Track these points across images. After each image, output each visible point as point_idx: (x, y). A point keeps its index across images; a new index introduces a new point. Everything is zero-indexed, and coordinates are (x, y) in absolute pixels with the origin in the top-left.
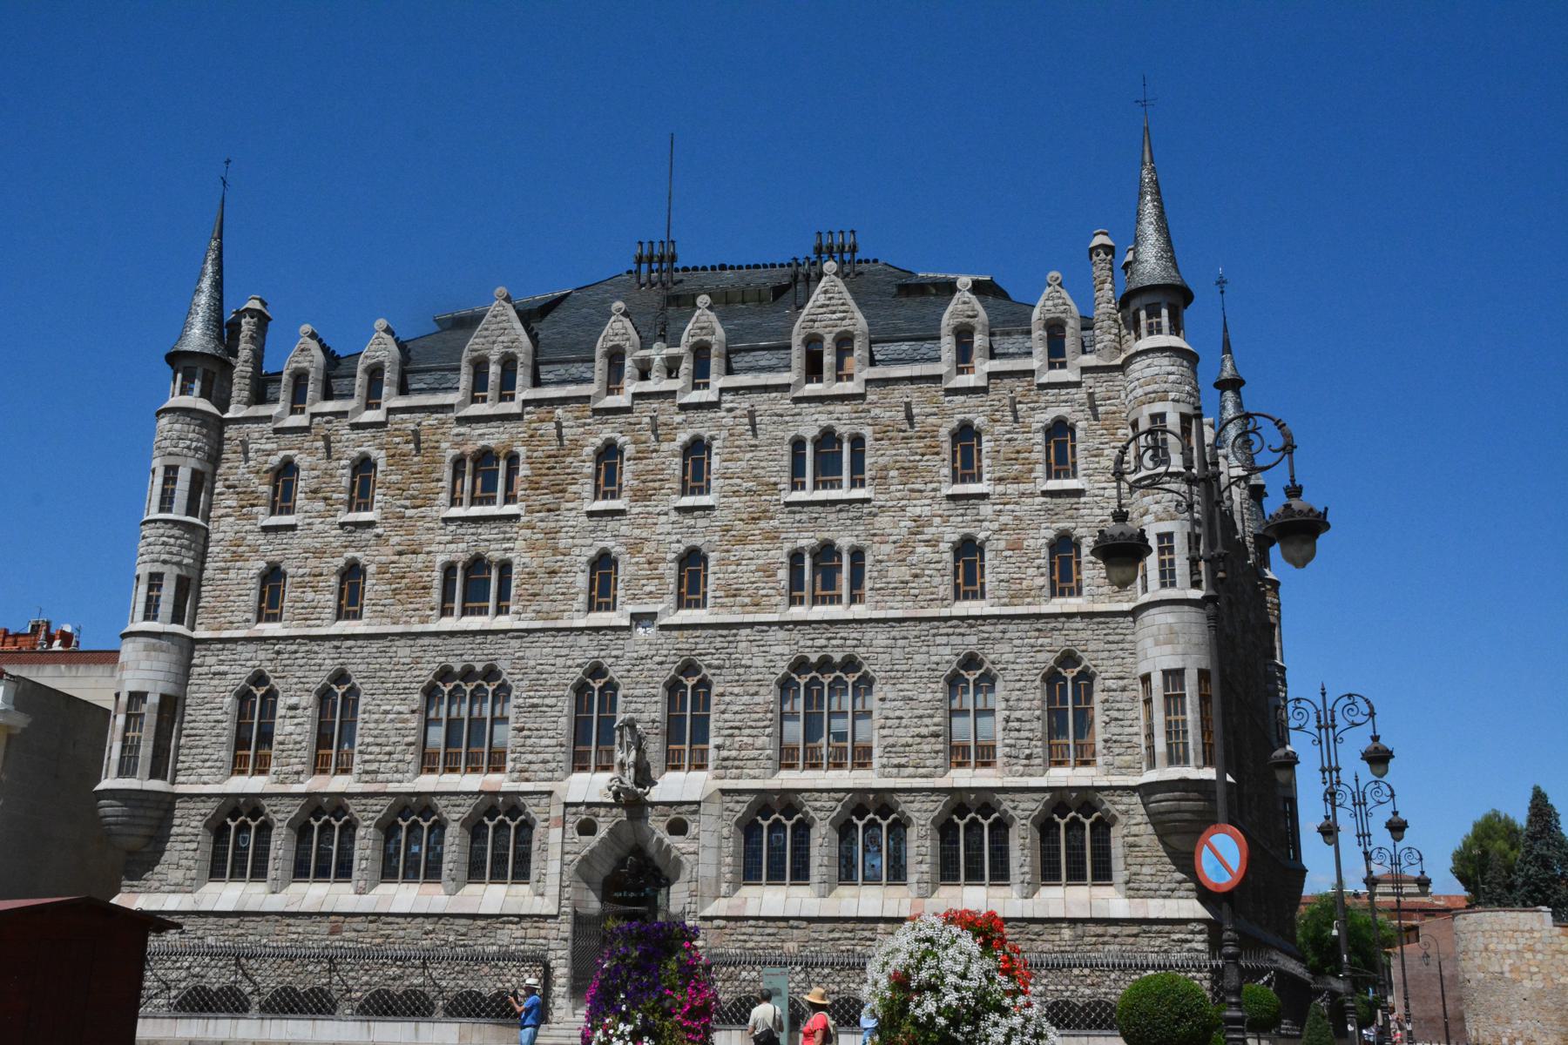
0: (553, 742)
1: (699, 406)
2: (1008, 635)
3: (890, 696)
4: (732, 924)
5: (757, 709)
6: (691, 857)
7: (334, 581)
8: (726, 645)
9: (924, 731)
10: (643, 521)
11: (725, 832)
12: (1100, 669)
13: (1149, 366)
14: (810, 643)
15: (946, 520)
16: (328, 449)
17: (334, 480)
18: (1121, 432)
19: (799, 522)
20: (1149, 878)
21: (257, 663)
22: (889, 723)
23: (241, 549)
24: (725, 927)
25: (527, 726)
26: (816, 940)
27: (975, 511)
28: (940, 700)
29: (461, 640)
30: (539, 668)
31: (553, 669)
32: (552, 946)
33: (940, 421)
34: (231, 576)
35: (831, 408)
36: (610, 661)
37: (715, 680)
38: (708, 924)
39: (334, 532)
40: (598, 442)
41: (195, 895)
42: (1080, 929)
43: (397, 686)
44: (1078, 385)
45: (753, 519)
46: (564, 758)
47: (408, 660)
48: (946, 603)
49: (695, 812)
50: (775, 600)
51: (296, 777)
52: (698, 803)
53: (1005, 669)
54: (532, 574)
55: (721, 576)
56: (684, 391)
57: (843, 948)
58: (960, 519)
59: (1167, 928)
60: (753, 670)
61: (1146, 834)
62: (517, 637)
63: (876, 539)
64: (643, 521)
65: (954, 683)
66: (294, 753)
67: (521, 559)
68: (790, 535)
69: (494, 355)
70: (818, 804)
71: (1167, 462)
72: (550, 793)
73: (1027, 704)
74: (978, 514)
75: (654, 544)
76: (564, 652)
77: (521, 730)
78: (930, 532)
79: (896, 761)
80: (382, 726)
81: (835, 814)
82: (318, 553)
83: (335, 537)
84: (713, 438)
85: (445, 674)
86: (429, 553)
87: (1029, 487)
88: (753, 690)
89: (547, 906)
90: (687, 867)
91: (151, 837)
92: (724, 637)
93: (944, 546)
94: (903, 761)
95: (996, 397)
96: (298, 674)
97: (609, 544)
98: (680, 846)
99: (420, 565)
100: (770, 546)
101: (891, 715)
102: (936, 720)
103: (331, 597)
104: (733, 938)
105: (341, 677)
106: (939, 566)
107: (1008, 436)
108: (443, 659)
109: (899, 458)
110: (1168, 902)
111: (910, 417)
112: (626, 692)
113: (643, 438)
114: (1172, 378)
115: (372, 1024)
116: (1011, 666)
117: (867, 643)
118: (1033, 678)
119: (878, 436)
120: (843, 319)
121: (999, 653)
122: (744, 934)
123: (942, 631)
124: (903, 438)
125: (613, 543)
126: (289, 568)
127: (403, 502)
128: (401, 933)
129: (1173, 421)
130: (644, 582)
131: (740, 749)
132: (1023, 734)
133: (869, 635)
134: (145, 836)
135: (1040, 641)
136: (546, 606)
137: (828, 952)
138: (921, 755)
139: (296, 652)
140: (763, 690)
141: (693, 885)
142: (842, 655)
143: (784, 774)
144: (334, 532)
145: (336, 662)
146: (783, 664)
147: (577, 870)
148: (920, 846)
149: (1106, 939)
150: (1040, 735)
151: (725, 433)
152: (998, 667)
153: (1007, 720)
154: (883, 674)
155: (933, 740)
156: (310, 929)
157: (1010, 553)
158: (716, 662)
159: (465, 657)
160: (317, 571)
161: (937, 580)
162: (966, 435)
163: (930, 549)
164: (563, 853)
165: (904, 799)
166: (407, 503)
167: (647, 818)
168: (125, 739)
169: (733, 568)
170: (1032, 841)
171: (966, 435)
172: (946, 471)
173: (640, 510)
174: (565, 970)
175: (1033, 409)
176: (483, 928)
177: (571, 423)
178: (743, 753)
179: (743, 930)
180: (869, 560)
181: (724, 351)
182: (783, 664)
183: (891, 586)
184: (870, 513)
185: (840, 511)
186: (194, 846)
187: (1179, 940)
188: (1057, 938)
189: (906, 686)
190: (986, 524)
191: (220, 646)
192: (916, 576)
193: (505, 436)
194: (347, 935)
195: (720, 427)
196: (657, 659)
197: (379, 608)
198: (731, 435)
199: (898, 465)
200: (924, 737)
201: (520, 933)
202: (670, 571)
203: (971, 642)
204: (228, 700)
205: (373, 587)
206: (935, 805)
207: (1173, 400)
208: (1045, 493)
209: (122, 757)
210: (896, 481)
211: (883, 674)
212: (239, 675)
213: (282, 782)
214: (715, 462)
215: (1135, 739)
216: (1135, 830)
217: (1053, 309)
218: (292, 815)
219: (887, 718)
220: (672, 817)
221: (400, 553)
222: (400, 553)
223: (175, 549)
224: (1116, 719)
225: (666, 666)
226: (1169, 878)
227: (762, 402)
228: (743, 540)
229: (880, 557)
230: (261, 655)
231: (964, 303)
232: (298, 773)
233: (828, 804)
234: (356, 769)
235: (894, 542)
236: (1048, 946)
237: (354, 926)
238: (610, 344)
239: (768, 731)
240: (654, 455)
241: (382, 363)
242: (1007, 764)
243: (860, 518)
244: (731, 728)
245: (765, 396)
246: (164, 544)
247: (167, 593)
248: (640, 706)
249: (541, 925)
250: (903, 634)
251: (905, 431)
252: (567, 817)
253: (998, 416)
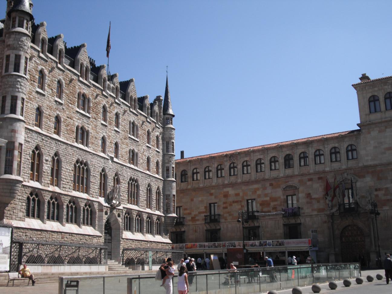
17: (54, 84)
21: (37, 141)
34: (29, 105)
36: (106, 168)
43: (70, 161)
62: (91, 155)
82: (50, 108)
83: (54, 105)
86: (74, 120)
92: (122, 167)
100: (127, 147)
108: (78, 156)
115: (91, 266)
121: (152, 184)
145: (57, 148)
156: (57, 237)
191: (28, 131)
194: (66, 239)
202: (113, 146)
213: (44, 186)
222: (68, 117)
228: (123, 143)
230: (39, 139)
232: (48, 184)
240: (111, 113)
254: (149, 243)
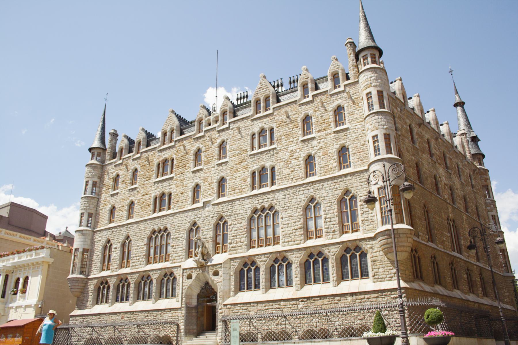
0: (182, 249)
1: (223, 130)
2: (324, 187)
3: (284, 216)
4: (233, 307)
5: (242, 228)
7: (126, 208)
8: (231, 207)
9: (296, 227)
10: (207, 171)
11: (232, 274)
12: (358, 193)
13: (364, 76)
14: (258, 202)
15: (301, 149)
16: (127, 168)
18: (360, 104)
19: (254, 161)
20: (382, 273)
21: (107, 236)
22: (284, 226)
23: (106, 202)
24: (231, 308)
25: (175, 245)
26: (260, 310)
27: (311, 144)
28: (301, 215)
29: (157, 220)
30: (178, 225)
31: (181, 225)
32: (179, 319)
33: (298, 116)
35: (263, 120)
36: (197, 219)
38: (225, 307)
39: (127, 193)
40: (195, 148)
41: (91, 309)
42: (354, 297)
43: (142, 237)
44: (344, 91)
45: (240, 163)
46: (184, 254)
47: (143, 229)
48: (302, 179)
49: (221, 267)
50: (246, 189)
51: (116, 270)
52: (221, 264)
53: (324, 199)
54: (177, 195)
55: (230, 184)
56: (219, 126)
57: (270, 312)
58: (306, 148)
59: (389, 293)
60: (240, 215)
61: (381, 256)
62: (172, 216)
63: (278, 161)
64: (207, 171)
65: (306, 208)
66: (115, 262)
67: (174, 190)
68: (251, 166)
69: (168, 130)
70: (261, 260)
71: (373, 109)
72: (180, 266)
73: (332, 211)
74: (312, 145)
75: (210, 178)
76: (185, 218)
77: (173, 246)
78: (296, 155)
79: (287, 240)
80: (137, 251)
81: (267, 262)
82: (123, 200)
84: (227, 139)
85: (154, 232)
86: (150, 194)
87: (329, 131)
88: (240, 222)
89: (178, 305)
91: (82, 292)
92: (230, 205)
93: (301, 159)
94: (289, 240)
95: (316, 103)
96: (117, 238)
97: (199, 181)
98: (216, 280)
99: (148, 198)
100: (245, 171)
101: (285, 223)
102: (300, 222)
103: (126, 212)
104: (233, 311)
105: (128, 237)
106: (300, 166)
107: (321, 115)
108: (152, 227)
109: (285, 132)
110: (390, 282)
111: (288, 117)
113: (207, 144)
114: (372, 78)
116: (326, 198)
117: (276, 199)
118: (334, 201)
119: (278, 126)
120: (266, 91)
122: (237, 310)
123: (301, 189)
124: (286, 124)
125: (199, 180)
126: (116, 206)
127: (144, 180)
128: (139, 317)
129: (374, 94)
130: (207, 191)
131: (236, 243)
132: (332, 223)
133: (276, 196)
134: (81, 292)
135: (335, 187)
136: (180, 204)
137: (264, 314)
138: (296, 237)
139: (117, 231)
140: (243, 221)
142: (268, 204)
143: (252, 250)
144: (127, 193)
146: (249, 211)
148: (296, 272)
149: (365, 300)
150: (337, 222)
151: (231, 137)
152: (321, 199)
153: (325, 218)
154: (282, 209)
155: (299, 230)
157: (324, 156)
158: (228, 214)
159: (158, 225)
160: (123, 205)
161: (299, 172)
162: (307, 119)
163: (296, 161)
165: (290, 254)
166: (145, 180)
168: (74, 263)
169: (234, 181)
170: (336, 264)
171: (307, 119)
172: (300, 132)
173: (206, 167)
175: (329, 104)
176: (161, 314)
177: (188, 145)
178: (237, 244)
179: (236, 308)
180: (276, 169)
181: (233, 111)
182: (249, 211)
183: (284, 177)
184: (276, 153)
185: (267, 154)
186: (91, 294)
187: (394, 298)
188: (346, 301)
189: (290, 212)
190: (314, 148)
192: (292, 171)
193: (170, 153)
194: (126, 319)
195: (229, 135)
196: (211, 216)
197: (138, 214)
198: (233, 137)
199: (284, 134)
200: (296, 229)
201: (170, 315)
202: (215, 186)
203: (311, 191)
204: (101, 248)
205: (136, 207)
206: (300, 255)
207: (374, 86)
208: (335, 132)
209: (73, 269)
210: (284, 140)
211: (282, 209)
212: (104, 240)
213: (113, 272)
214: (228, 147)
215: (373, 218)
216: (375, 254)
217: (334, 68)
218: (114, 282)
219: (284, 225)
220: (215, 269)
221: (143, 196)
222: (143, 196)
223: (87, 205)
224: (366, 212)
225: (214, 218)
226: (389, 272)
227: (241, 124)
228: (236, 171)
229: (280, 167)
230: (109, 233)
231: (304, 74)
232: (116, 268)
233: (264, 259)
234: (131, 265)
235: (284, 161)
236: (342, 305)
237: (127, 316)
238: (199, 117)
239: (245, 235)
241: (141, 139)
242: (326, 235)
243: (273, 155)
244: (234, 236)
245: (243, 122)
246: (85, 204)
247: (85, 218)
248: (206, 233)
249: (176, 312)
250: (288, 193)
251: (286, 122)
253: (317, 109)
254: (302, 301)
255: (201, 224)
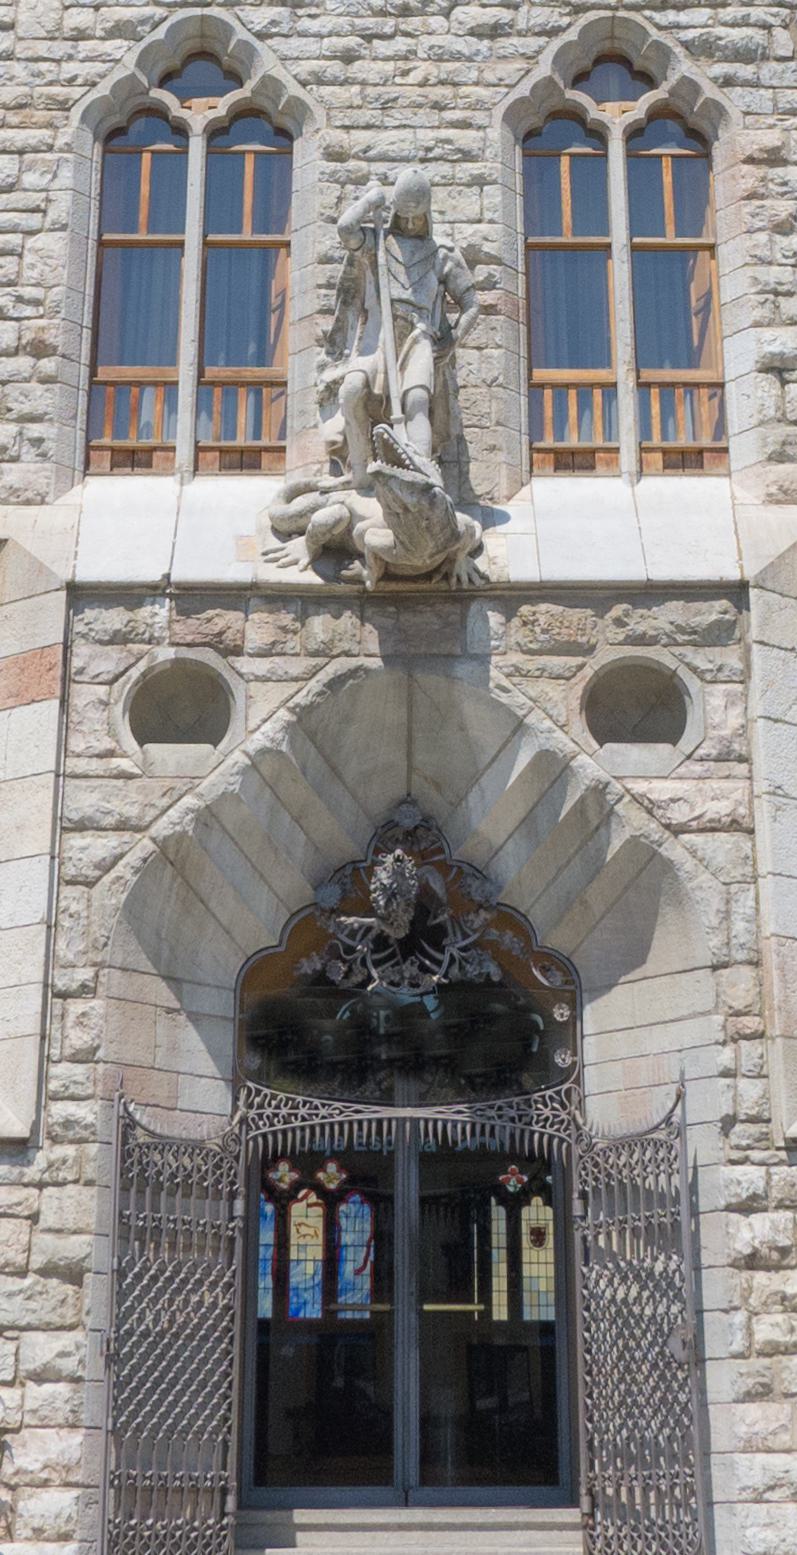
6: (718, 847)
37: (734, 101)
90: (705, 890)
112: (338, 137)
141: (740, 986)
147: (134, 911)
158: (736, 35)
164: (66, 826)
167: (483, 659)
174: (68, 1445)
220: (606, 656)
252: (82, 654)
255: (320, 80)
